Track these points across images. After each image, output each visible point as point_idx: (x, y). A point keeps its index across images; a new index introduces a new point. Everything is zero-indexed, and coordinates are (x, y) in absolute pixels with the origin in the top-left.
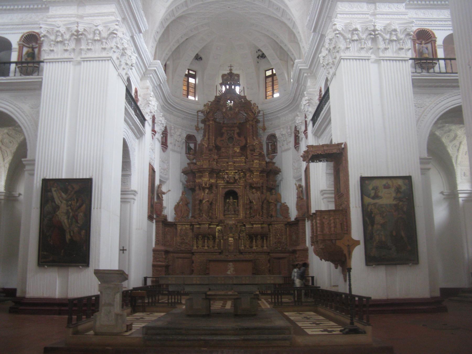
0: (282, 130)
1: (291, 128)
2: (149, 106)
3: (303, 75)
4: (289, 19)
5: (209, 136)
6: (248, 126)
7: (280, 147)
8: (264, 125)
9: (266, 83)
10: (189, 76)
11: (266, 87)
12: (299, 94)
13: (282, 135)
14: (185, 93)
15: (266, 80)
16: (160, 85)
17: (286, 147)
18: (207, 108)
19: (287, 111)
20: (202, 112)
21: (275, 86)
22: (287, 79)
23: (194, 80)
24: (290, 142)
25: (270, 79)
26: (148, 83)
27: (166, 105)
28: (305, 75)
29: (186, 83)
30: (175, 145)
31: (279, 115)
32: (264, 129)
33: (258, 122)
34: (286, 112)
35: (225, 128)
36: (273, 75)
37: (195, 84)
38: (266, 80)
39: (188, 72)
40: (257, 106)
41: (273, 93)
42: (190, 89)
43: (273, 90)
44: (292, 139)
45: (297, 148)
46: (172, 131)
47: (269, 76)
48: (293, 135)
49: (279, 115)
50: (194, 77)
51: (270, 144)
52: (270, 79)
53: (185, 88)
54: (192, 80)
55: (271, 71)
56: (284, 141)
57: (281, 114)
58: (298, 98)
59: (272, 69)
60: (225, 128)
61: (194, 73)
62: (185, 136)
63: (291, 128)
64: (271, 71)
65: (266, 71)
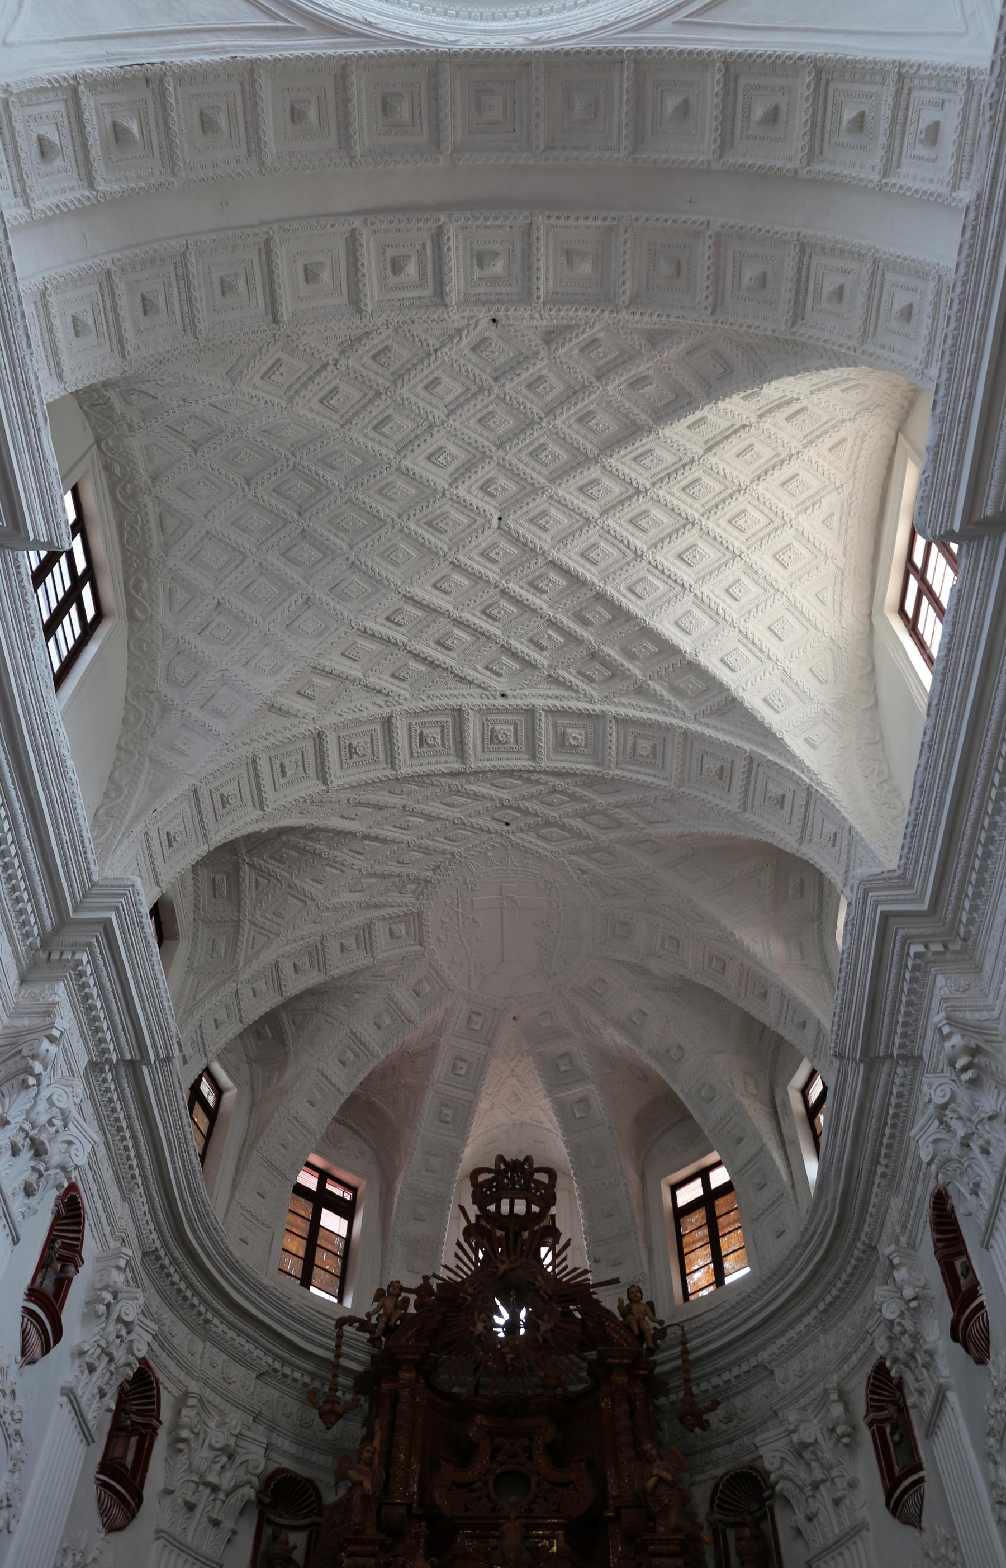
0: (792, 1416)
1: (843, 1397)
2: (25, 1086)
3: (904, 954)
4: (781, 801)
5: (389, 1443)
6: (605, 1403)
7: (799, 1532)
8: (689, 1393)
9: (679, 1237)
10: (321, 1199)
11: (682, 1256)
12: (875, 1162)
13: (801, 1450)
14: (294, 1266)
15: (678, 1226)
16: (133, 1067)
17: (831, 1525)
18: (390, 1303)
19: (808, 1319)
20: (364, 1325)
21: (723, 1241)
22: (785, 1177)
23: (345, 1223)
24: (852, 1485)
25: (698, 1217)
26: (60, 993)
27: (174, 1261)
28: (914, 949)
29: (303, 1228)
30: (191, 1507)
31: (764, 1356)
32: (693, 1416)
33: (655, 1386)
34: (800, 1327)
35: (480, 1419)
36: (710, 1197)
37: (348, 1240)
38: (678, 1226)
39: (321, 1184)
40: (651, 1305)
41: (720, 1274)
42: (322, 1257)
43: (718, 1259)
44: (865, 1468)
45: (911, 1501)
46: (188, 1415)
47: (693, 1206)
48: (865, 1436)
49: (764, 1356)
50: (346, 1210)
51: (731, 1535)
52: (698, 1217)
53: (298, 1246)
54: (331, 1221)
55: (699, 1182)
56: (815, 1486)
57: (773, 1348)
58: (868, 1192)
59: (704, 1174)
60: (480, 1419)
61: (348, 1196)
62: (256, 1458)
63: (843, 1397)
64: (699, 1182)
65: (675, 1188)
